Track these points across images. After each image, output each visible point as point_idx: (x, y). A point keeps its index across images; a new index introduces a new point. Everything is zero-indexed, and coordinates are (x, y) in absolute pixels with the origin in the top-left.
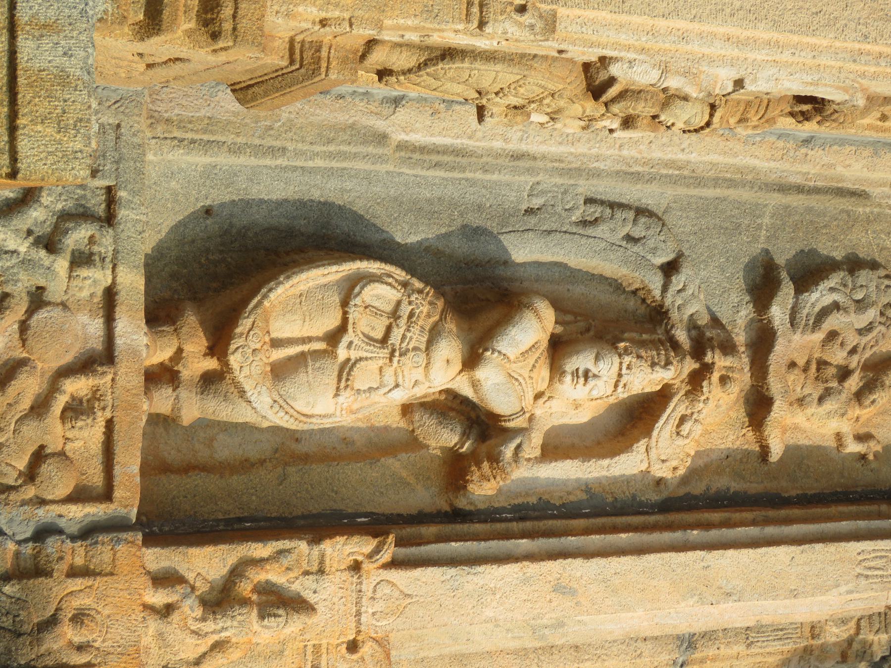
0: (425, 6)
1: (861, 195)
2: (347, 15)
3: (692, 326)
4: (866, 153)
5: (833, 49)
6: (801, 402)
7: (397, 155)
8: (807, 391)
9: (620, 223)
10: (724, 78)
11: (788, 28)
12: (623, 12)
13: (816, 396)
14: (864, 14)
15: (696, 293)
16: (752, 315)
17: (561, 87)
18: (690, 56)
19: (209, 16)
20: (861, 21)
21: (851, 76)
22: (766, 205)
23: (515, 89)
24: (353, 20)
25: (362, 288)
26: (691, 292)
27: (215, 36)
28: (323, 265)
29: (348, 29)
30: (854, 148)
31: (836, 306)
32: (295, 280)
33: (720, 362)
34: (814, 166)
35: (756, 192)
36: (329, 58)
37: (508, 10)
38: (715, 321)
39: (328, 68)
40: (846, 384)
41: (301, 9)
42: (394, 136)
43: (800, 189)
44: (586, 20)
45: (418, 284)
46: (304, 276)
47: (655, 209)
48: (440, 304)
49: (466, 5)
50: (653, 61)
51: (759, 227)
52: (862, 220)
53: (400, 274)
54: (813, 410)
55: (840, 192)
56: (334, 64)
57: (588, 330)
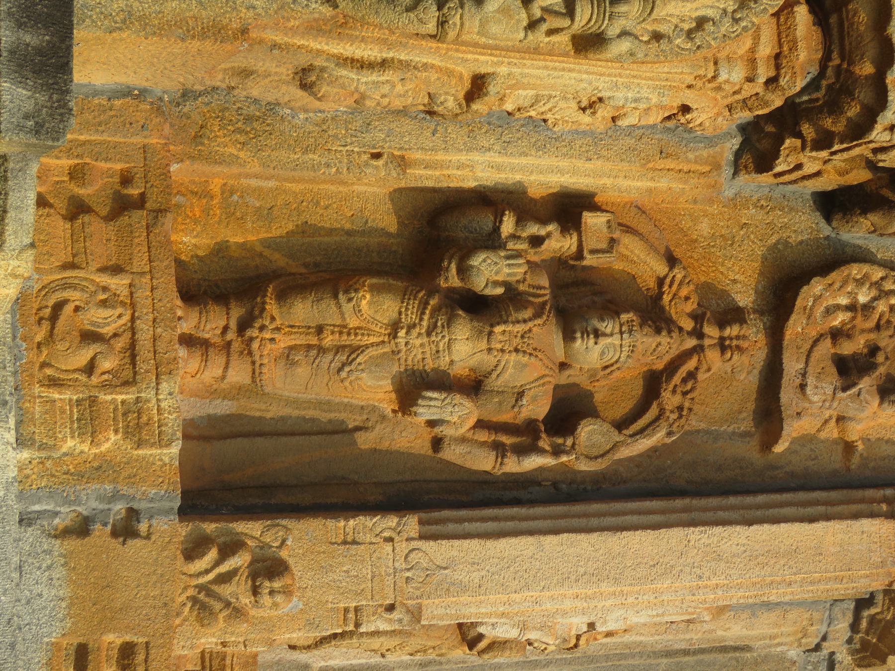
0: (308, 620)
1: (744, 649)
2: (241, 639)
4: (744, 616)
5: (673, 588)
10: (579, 623)
11: (628, 582)
12: (479, 595)
14: (698, 559)
17: (439, 643)
18: (546, 613)
19: (126, 662)
20: (695, 564)
21: (693, 604)
22: (659, 664)
23: (400, 648)
24: (246, 643)
29: (243, 649)
30: (732, 613)
34: (696, 634)
35: (645, 660)
36: (232, 665)
37: (379, 611)
41: (203, 641)
42: (315, 665)
43: (686, 652)
44: (450, 603)
49: (343, 612)
50: (512, 622)
52: (750, 664)
55: (724, 649)
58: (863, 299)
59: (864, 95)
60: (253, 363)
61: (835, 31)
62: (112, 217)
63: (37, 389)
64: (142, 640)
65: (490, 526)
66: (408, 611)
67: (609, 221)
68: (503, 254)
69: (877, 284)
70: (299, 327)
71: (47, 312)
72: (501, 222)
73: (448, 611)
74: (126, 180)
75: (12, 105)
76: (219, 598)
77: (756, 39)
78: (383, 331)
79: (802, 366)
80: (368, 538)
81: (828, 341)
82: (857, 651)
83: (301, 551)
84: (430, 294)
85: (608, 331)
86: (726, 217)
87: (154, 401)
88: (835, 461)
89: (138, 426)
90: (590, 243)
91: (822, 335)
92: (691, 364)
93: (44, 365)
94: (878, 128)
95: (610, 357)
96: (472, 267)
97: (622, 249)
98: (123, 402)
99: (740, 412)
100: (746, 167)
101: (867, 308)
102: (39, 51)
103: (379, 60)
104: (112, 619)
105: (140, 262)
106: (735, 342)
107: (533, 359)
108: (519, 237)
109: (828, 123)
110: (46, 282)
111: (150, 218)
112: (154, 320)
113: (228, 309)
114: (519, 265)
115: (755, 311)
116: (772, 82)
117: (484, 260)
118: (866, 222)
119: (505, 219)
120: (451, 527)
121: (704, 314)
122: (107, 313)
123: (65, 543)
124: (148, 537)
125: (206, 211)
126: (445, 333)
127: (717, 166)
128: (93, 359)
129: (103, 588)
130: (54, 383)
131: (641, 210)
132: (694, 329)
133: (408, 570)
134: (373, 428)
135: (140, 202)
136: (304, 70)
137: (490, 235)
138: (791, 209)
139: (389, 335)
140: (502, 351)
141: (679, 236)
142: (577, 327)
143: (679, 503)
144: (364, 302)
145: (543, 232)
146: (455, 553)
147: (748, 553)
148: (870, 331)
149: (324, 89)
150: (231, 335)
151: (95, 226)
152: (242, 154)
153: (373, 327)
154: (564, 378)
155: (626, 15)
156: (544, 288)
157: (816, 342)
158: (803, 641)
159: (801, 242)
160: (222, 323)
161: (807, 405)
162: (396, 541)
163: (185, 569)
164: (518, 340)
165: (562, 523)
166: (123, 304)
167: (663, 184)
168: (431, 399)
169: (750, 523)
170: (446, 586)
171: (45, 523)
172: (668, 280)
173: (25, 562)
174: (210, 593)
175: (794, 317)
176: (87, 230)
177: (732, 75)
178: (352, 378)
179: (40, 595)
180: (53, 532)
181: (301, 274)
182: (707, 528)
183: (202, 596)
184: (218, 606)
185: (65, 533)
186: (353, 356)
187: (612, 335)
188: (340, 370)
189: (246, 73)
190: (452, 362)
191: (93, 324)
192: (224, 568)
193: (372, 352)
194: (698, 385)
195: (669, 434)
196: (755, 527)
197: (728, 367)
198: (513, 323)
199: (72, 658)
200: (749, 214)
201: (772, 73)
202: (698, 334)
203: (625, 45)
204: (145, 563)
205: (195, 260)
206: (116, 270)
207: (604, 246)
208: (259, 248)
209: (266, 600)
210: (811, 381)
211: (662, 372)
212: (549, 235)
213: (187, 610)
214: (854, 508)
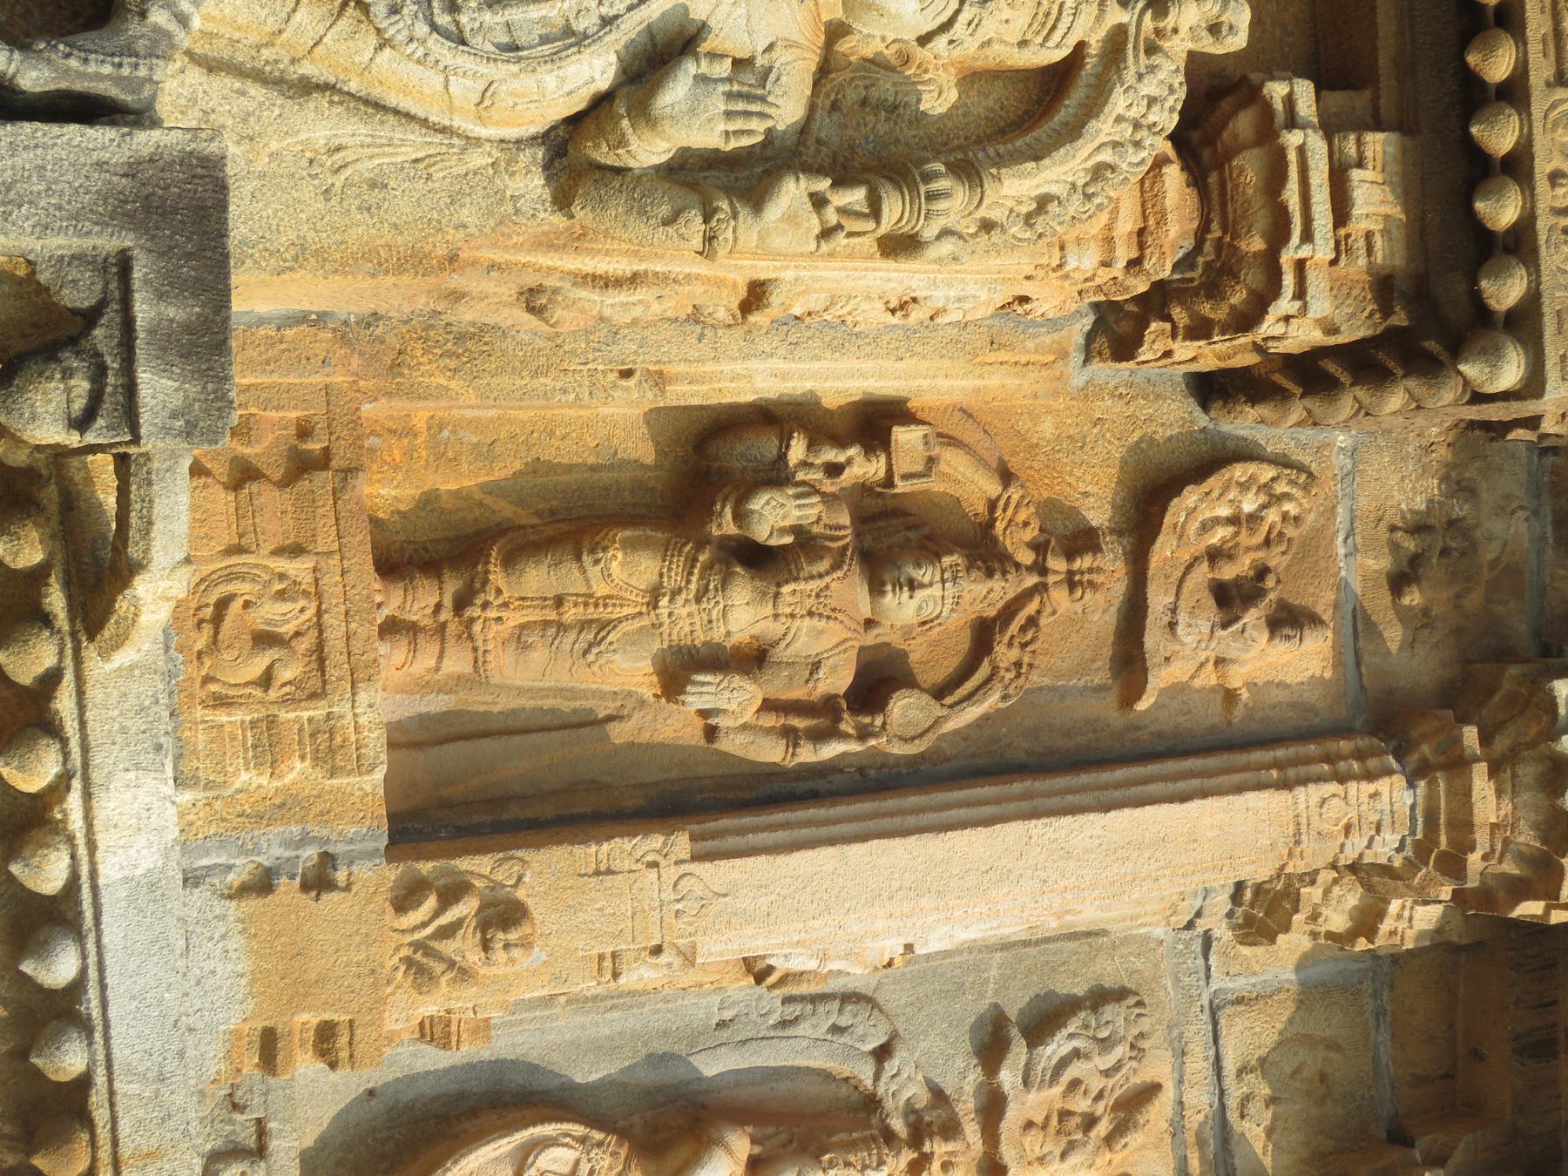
2: (470, 1005)
3: (910, 1110)
6: (1041, 1160)
7: (568, 1008)
8: (1046, 1150)
9: (823, 1017)
13: (1057, 1152)
15: (913, 1075)
16: (981, 1078)
25: (536, 1157)
26: (906, 1076)
27: (333, 1066)
28: (494, 1140)
31: (1076, 1054)
32: (463, 1162)
33: (938, 1148)
38: (939, 1096)
39: (458, 1041)
40: (1093, 1134)
41: (421, 1010)
45: (598, 1136)
46: (472, 1157)
47: (864, 991)
48: (623, 1152)
51: (987, 981)
53: (578, 1130)
54: (1056, 1167)
55: (1074, 936)
56: (464, 1036)
57: (791, 1141)
58: (1248, 507)
59: (1252, 277)
60: (475, 649)
61: (1215, 195)
62: (287, 481)
63: (199, 713)
64: (345, 1018)
65: (781, 836)
66: (680, 952)
67: (925, 436)
68: (791, 492)
69: (1266, 488)
70: (532, 599)
71: (208, 612)
72: (788, 447)
73: (730, 947)
74: (304, 432)
75: (154, 402)
76: (439, 957)
77: (1115, 212)
78: (640, 599)
79: (1171, 599)
80: (628, 864)
81: (1205, 565)
82: (1240, 927)
83: (542, 889)
84: (700, 546)
85: (926, 580)
86: (1075, 412)
87: (350, 716)
88: (1213, 714)
89: (331, 751)
90: (903, 465)
91: (1196, 559)
92: (1032, 608)
93: (207, 680)
94: (1270, 319)
95: (927, 613)
96: (752, 512)
97: (943, 467)
98: (310, 720)
99: (1094, 661)
100: (1100, 353)
101: (1254, 518)
102: (188, 328)
103: (629, 274)
104: (306, 995)
105: (326, 539)
106: (1086, 577)
107: (831, 623)
108: (812, 465)
109: (1206, 309)
110: (205, 573)
111: (337, 480)
112: (347, 613)
113: (441, 582)
114: (812, 505)
115: (1112, 531)
116: (1135, 264)
117: (768, 503)
118: (1252, 412)
119: (793, 443)
120: (731, 842)
121: (1048, 542)
122: (286, 607)
123: (243, 904)
124: (348, 888)
125: (409, 454)
126: (720, 598)
127: (1063, 355)
128: (270, 669)
129: (293, 957)
130: (221, 702)
131: (966, 413)
132: (1035, 562)
133: (678, 901)
134: (630, 716)
135: (323, 461)
136: (531, 290)
137: (774, 463)
138: (1158, 396)
139: (648, 604)
140: (793, 616)
141: (1016, 441)
142: (887, 577)
143: (1017, 787)
144: (615, 564)
145: (841, 458)
146: (736, 875)
147: (1104, 847)
148: (1258, 548)
149: (558, 314)
150: (445, 615)
151: (266, 496)
152: (453, 384)
153: (627, 595)
154: (871, 639)
155: (946, 212)
156: (844, 527)
157: (1189, 568)
158: (1172, 918)
159: (1170, 438)
160: (434, 600)
161: (1178, 647)
162: (661, 866)
163: (396, 925)
164: (812, 600)
165: (871, 825)
166: (306, 594)
167: (996, 381)
168: (703, 684)
169: (1106, 808)
170: (726, 917)
171: (216, 881)
172: (1001, 503)
173: (192, 932)
174: (429, 952)
175: (1161, 539)
176: (255, 503)
177: (1084, 261)
178: (602, 661)
179: (213, 972)
180: (226, 892)
181: (533, 526)
182: (1053, 819)
183: (418, 956)
184: (438, 968)
185: (243, 891)
186: (603, 633)
187: (931, 584)
188: (586, 652)
189: (457, 296)
190: (728, 633)
191: (269, 622)
192: (445, 919)
193: (627, 627)
194: (1042, 637)
195: (1005, 698)
196: (1113, 814)
197: (1078, 607)
198: (806, 580)
199: (257, 1046)
200: (1105, 407)
201: (1134, 254)
202: (1043, 571)
203: (947, 247)
204: (345, 921)
205: (396, 517)
206: (296, 551)
207: (919, 468)
208: (478, 496)
209: (500, 955)
210: (1182, 618)
211: (994, 619)
212: (849, 462)
213: (400, 974)
214: (1236, 778)
